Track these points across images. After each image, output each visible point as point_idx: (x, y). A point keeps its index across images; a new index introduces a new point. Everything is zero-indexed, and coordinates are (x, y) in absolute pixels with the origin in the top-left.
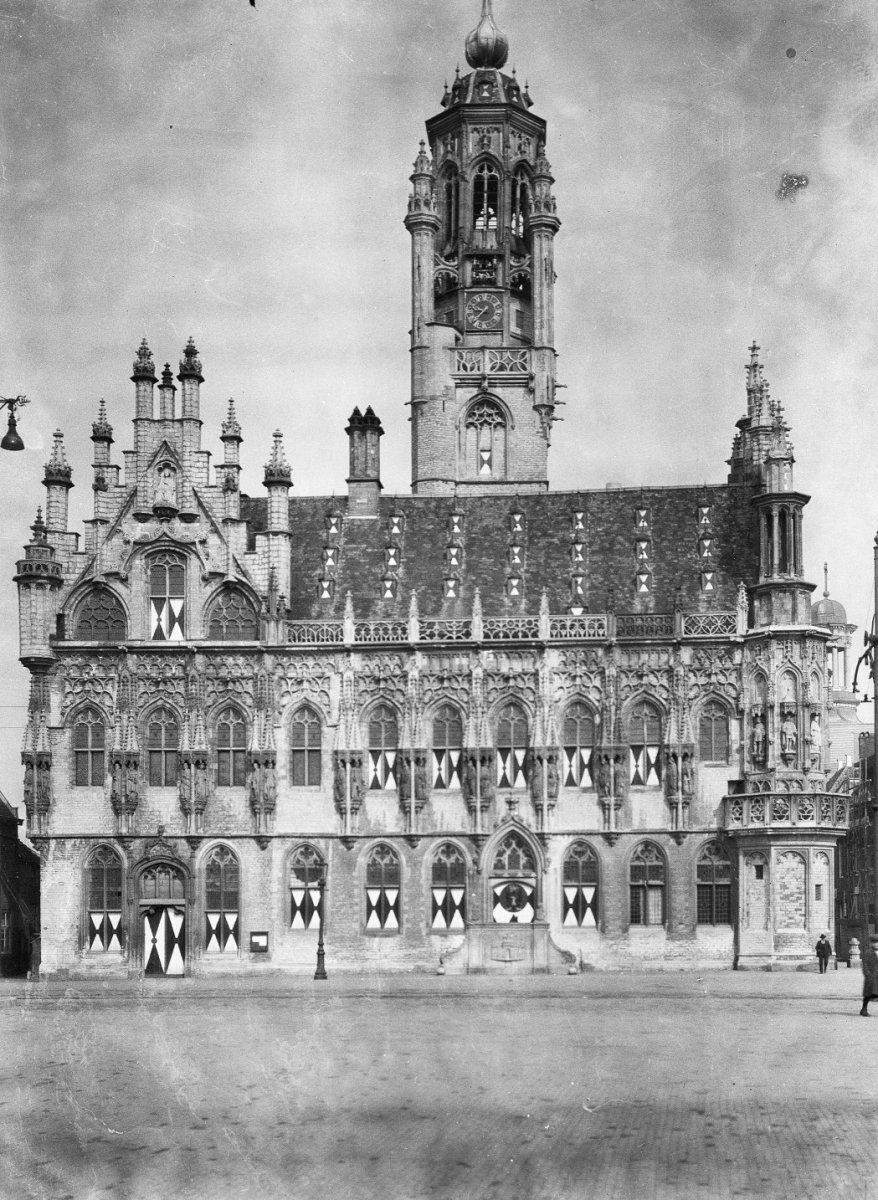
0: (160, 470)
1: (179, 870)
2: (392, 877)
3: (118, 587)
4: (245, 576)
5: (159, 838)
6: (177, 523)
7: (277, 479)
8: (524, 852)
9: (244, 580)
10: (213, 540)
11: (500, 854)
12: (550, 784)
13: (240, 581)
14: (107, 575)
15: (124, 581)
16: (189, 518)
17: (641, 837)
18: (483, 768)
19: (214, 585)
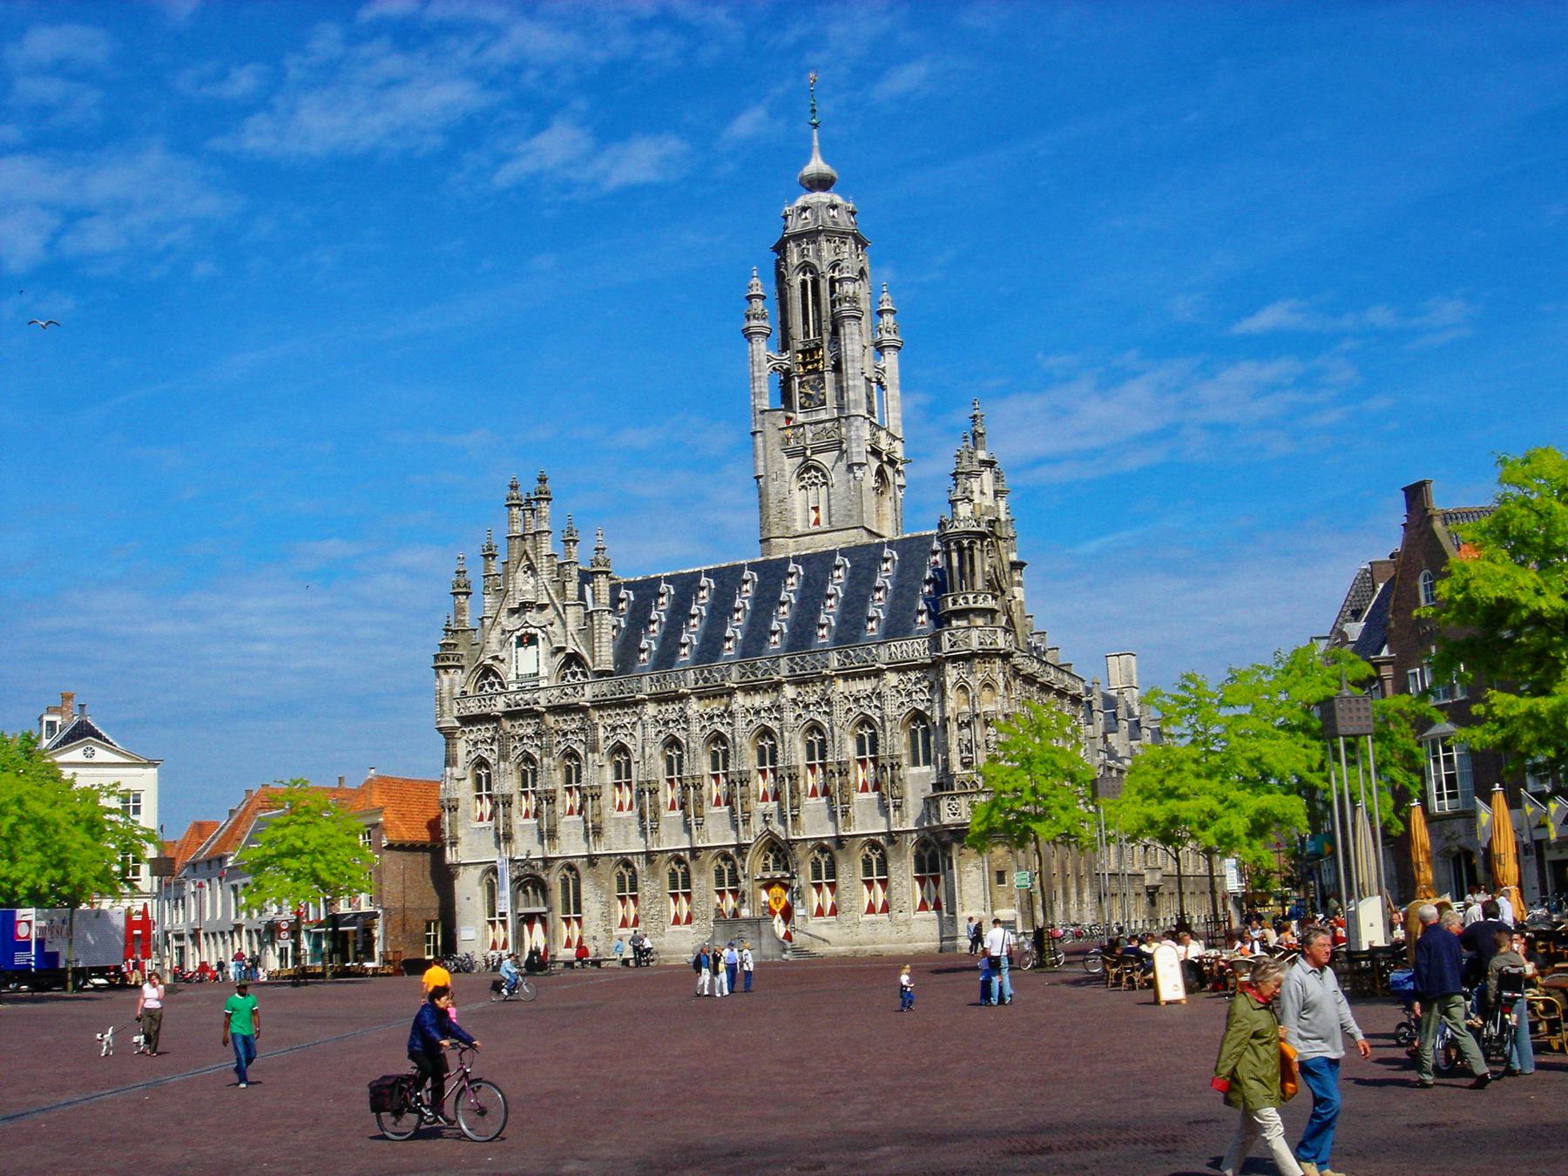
1: (541, 886)
3: (497, 666)
5: (527, 862)
10: (557, 622)
12: (792, 797)
16: (542, 607)
19: (561, 656)
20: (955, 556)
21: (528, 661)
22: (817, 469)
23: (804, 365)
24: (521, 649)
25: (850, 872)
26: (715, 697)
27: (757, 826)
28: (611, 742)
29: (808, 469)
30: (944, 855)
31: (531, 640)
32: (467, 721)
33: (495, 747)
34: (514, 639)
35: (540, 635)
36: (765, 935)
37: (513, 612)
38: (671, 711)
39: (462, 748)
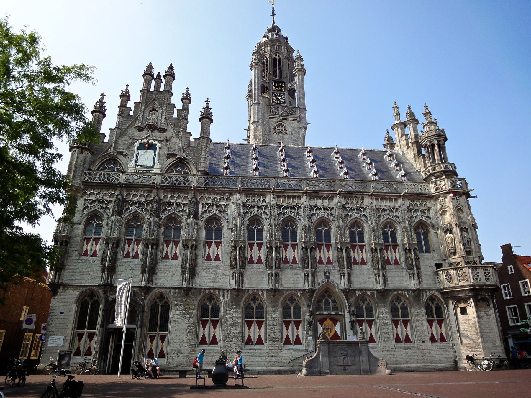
0: (151, 111)
2: (261, 313)
4: (187, 156)
6: (156, 133)
7: (206, 118)
8: (332, 300)
9: (187, 158)
11: (319, 301)
12: (347, 262)
13: (185, 159)
14: (118, 152)
15: (125, 156)
16: (163, 130)
17: (396, 293)
18: (312, 253)
19: (171, 160)
20: (436, 146)
21: (146, 158)
22: (282, 126)
23: (276, 87)
24: (140, 151)
25: (383, 315)
26: (289, 197)
27: (321, 279)
28: (206, 216)
29: (278, 126)
30: (456, 307)
31: (151, 147)
32: (89, 185)
33: (111, 207)
34: (137, 144)
35: (158, 145)
36: (364, 354)
37: (140, 129)
38: (256, 201)
39: (80, 203)
